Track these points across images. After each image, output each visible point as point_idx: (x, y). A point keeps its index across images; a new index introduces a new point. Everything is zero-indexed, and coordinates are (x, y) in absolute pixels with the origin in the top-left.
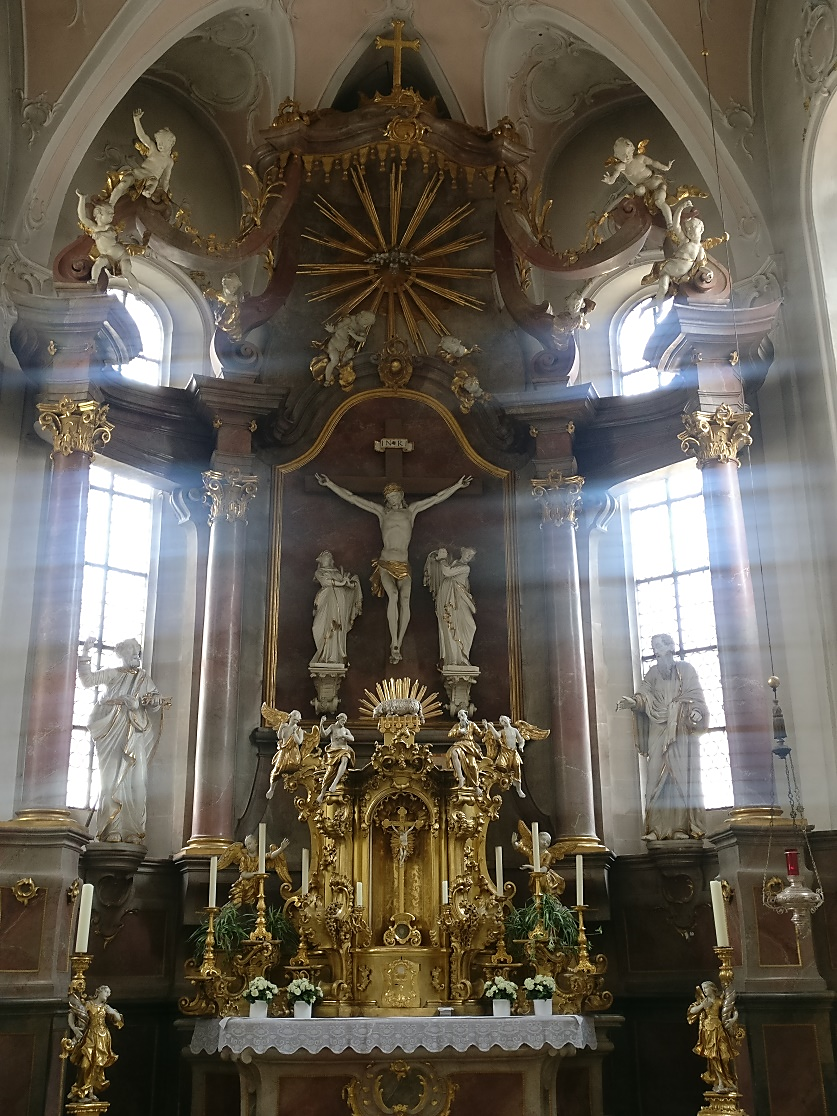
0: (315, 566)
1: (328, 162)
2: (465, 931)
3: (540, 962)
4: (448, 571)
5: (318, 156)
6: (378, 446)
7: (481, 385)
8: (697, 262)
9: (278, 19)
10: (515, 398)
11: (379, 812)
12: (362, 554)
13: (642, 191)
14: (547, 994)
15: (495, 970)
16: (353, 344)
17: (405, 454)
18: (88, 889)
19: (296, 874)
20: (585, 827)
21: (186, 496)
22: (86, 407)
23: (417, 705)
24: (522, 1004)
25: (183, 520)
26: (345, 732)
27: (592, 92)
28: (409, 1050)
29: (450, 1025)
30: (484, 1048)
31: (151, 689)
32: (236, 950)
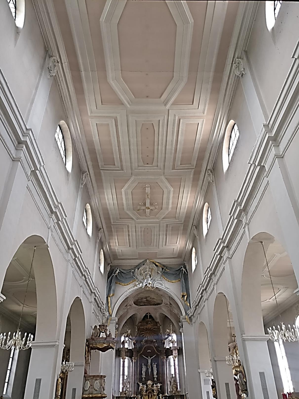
9: (138, 313)
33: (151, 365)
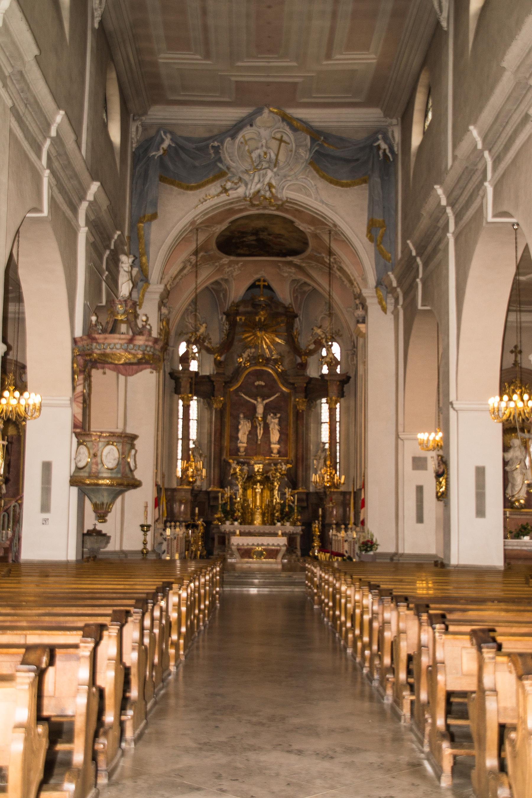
16: (249, 356)
33: (264, 418)
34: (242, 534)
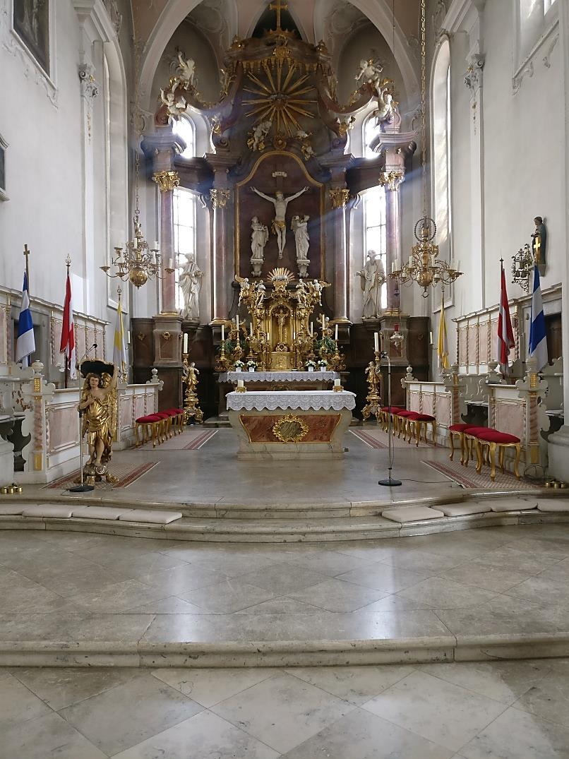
0: (252, 223)
1: (252, 63)
2: (301, 348)
3: (323, 356)
4: (299, 225)
5: (248, 62)
6: (274, 175)
7: (312, 149)
8: (389, 112)
10: (324, 160)
11: (273, 311)
12: (268, 219)
13: (370, 81)
14: (325, 365)
15: (310, 359)
16: (263, 134)
17: (284, 178)
18: (186, 335)
19: (248, 329)
20: (343, 315)
21: (204, 197)
22: (171, 174)
23: (286, 277)
24: (316, 368)
25: (204, 207)
26: (262, 286)
27: (359, 20)
28: (283, 381)
29: (295, 374)
30: (305, 380)
31: (198, 269)
32: (231, 352)
34: (251, 386)
